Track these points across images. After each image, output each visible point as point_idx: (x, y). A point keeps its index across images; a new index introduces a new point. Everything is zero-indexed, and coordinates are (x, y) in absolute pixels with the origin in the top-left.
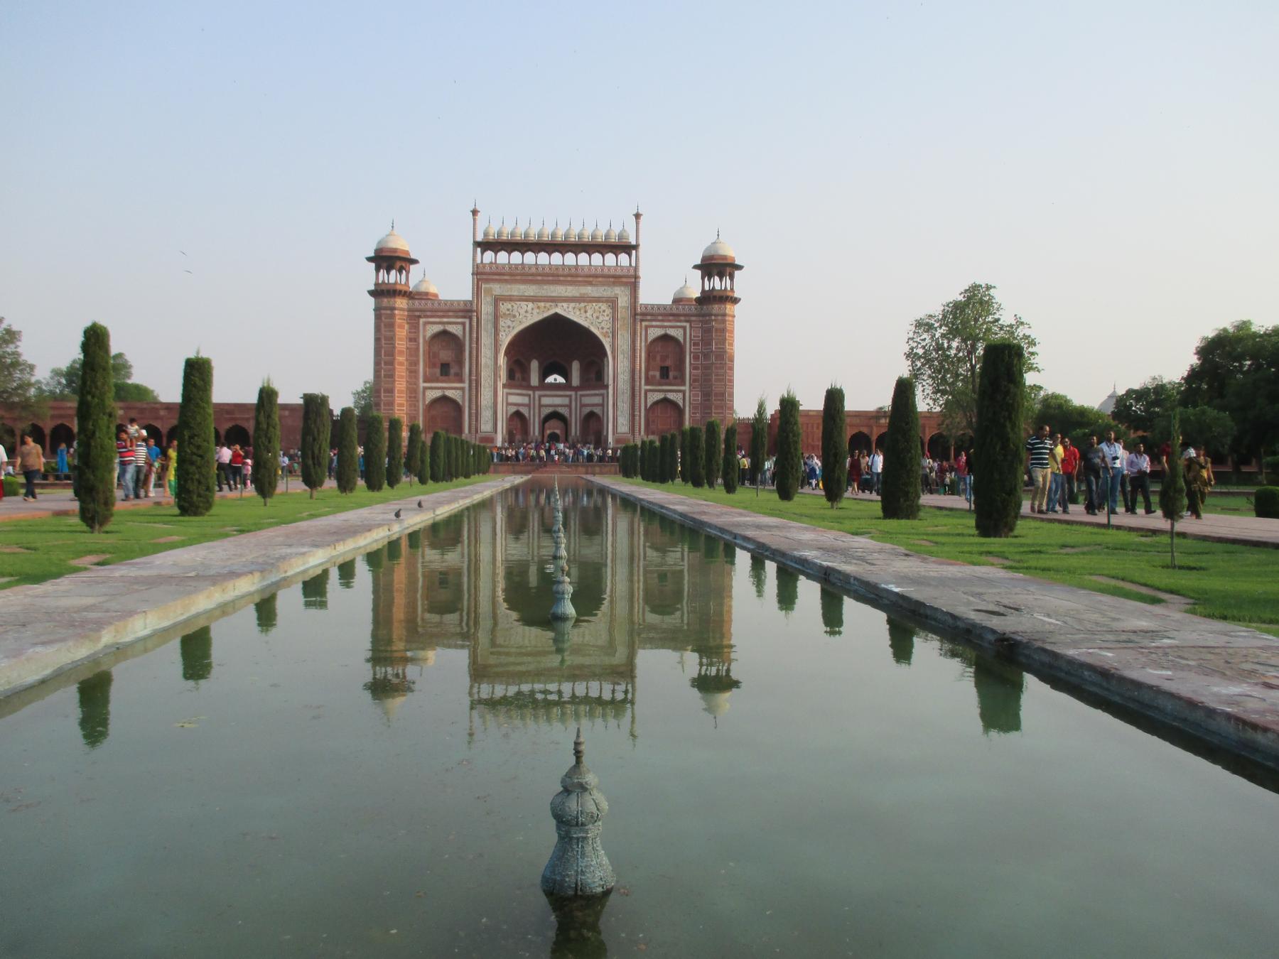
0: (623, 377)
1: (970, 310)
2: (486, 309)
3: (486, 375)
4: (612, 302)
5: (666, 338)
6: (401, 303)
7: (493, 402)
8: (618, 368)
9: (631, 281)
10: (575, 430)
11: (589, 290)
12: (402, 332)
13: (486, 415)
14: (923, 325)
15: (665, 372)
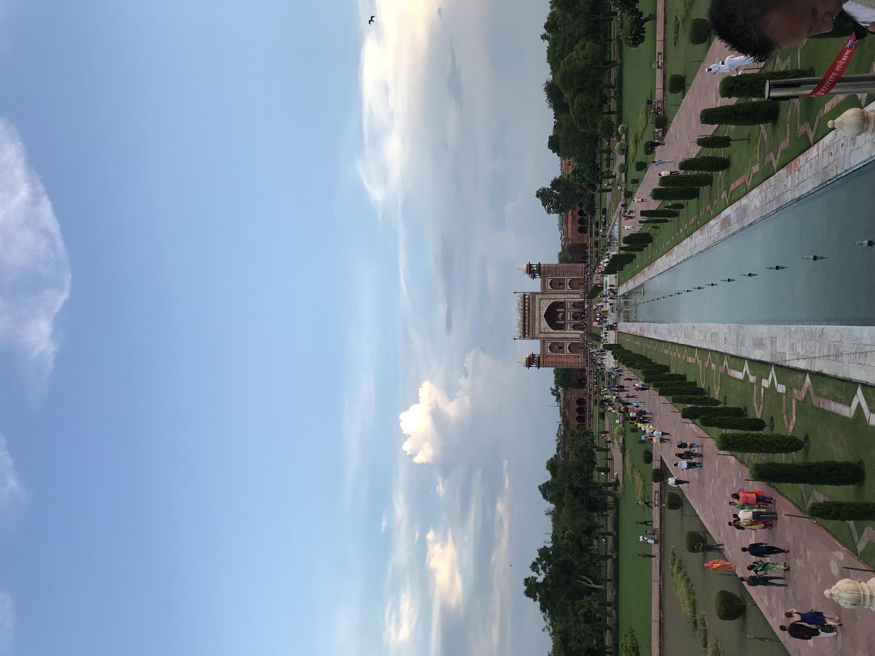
0: (562, 296)
1: (543, 195)
2: (543, 335)
3: (562, 336)
4: (540, 300)
5: (550, 284)
6: (541, 360)
7: (571, 334)
8: (560, 298)
9: (534, 294)
10: (578, 310)
11: (537, 307)
12: (550, 360)
13: (574, 336)
14: (549, 212)
15: (561, 284)
